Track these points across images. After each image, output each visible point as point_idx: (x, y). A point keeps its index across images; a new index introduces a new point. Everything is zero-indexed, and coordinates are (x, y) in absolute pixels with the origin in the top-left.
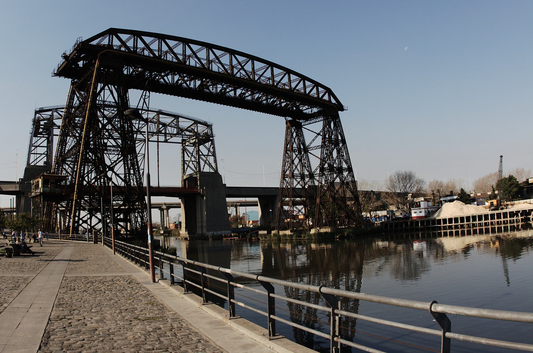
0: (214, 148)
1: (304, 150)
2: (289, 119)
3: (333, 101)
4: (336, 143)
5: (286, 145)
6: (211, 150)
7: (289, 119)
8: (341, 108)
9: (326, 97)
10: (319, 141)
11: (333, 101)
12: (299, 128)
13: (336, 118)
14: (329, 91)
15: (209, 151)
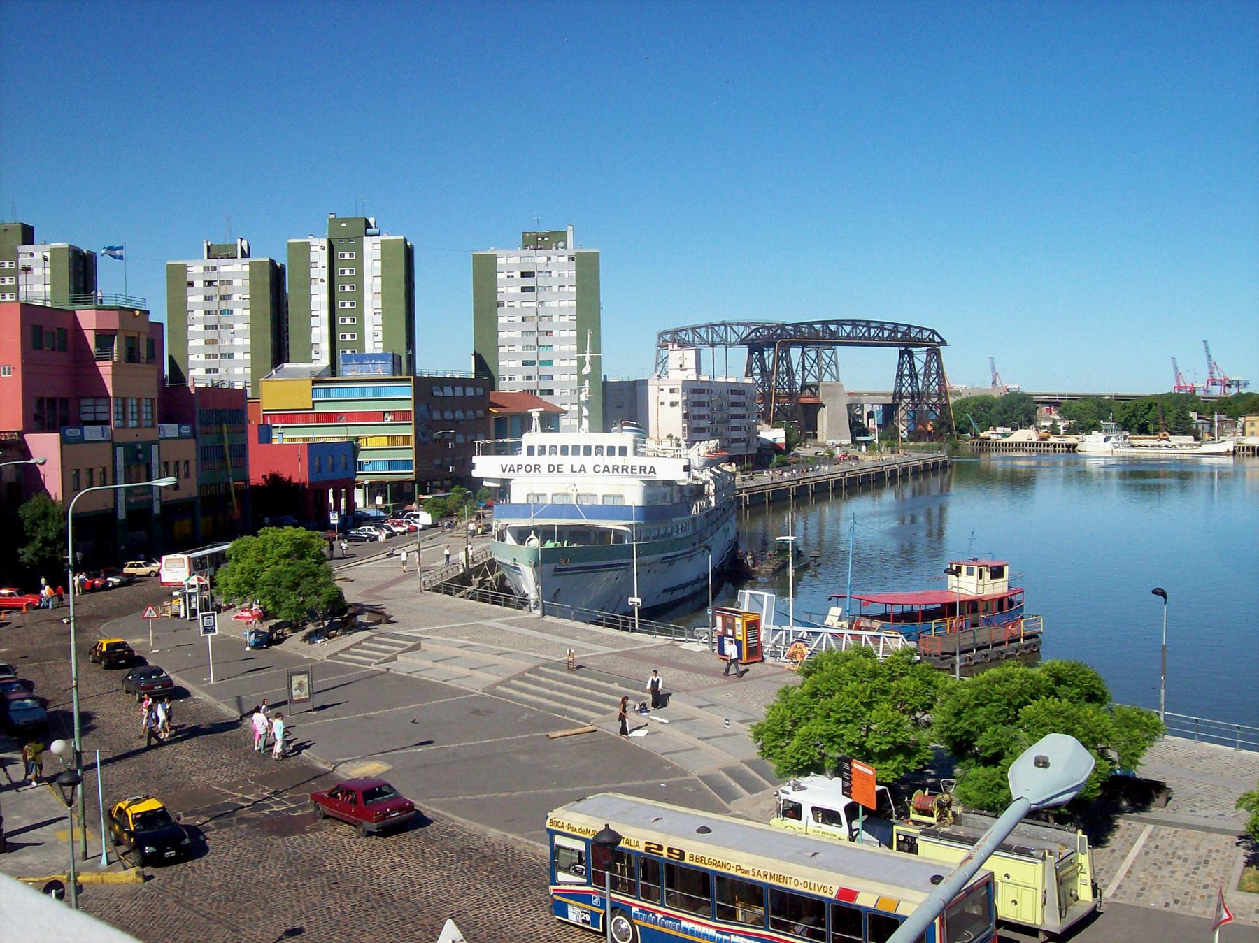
0: (836, 357)
1: (913, 375)
2: (903, 349)
3: (937, 339)
4: (938, 374)
5: (898, 372)
6: (833, 358)
7: (903, 349)
8: (943, 343)
9: (931, 337)
10: (922, 371)
11: (937, 339)
12: (911, 355)
13: (938, 354)
14: (933, 332)
15: (831, 360)
